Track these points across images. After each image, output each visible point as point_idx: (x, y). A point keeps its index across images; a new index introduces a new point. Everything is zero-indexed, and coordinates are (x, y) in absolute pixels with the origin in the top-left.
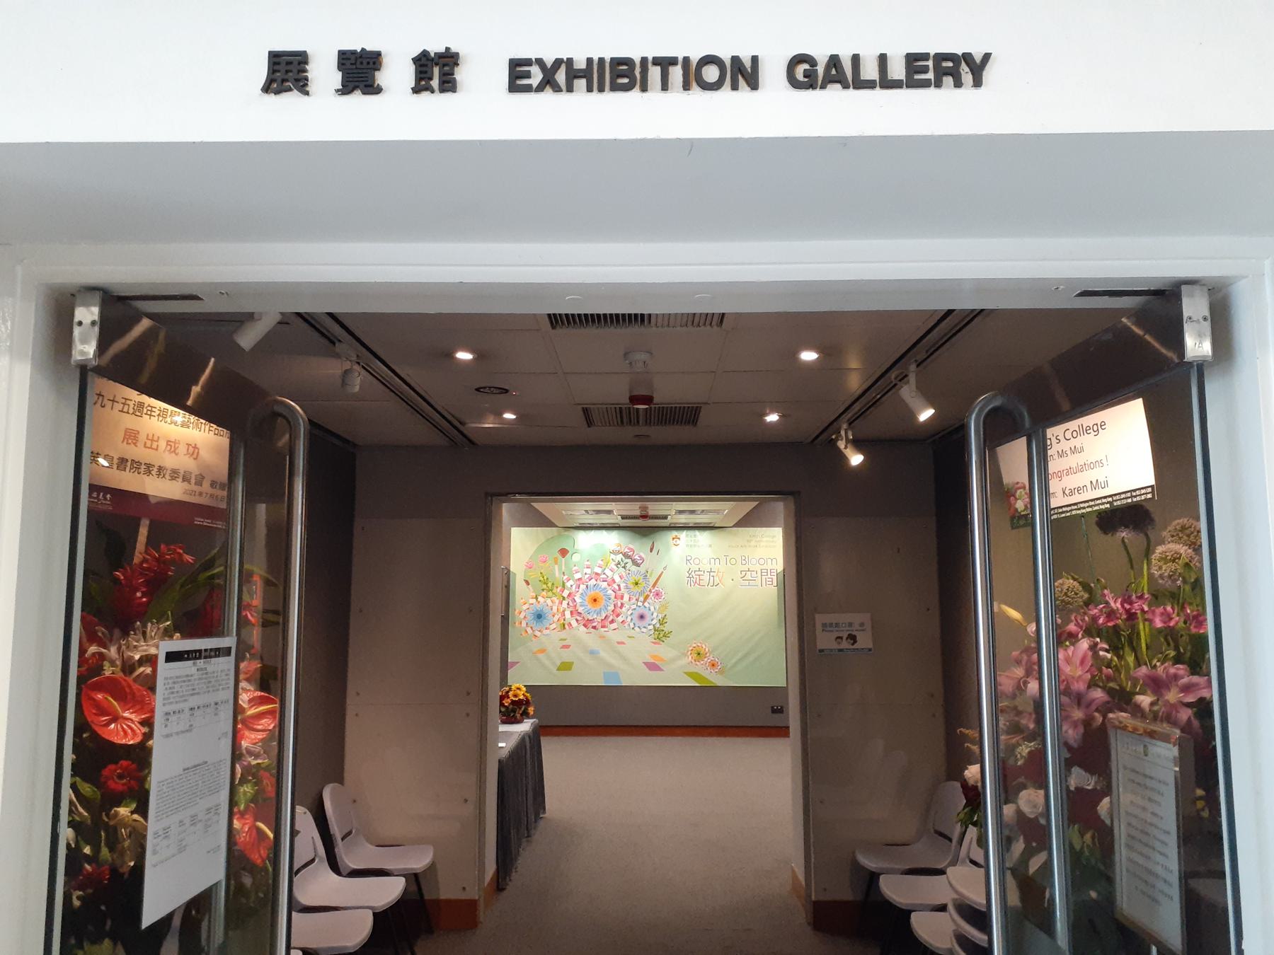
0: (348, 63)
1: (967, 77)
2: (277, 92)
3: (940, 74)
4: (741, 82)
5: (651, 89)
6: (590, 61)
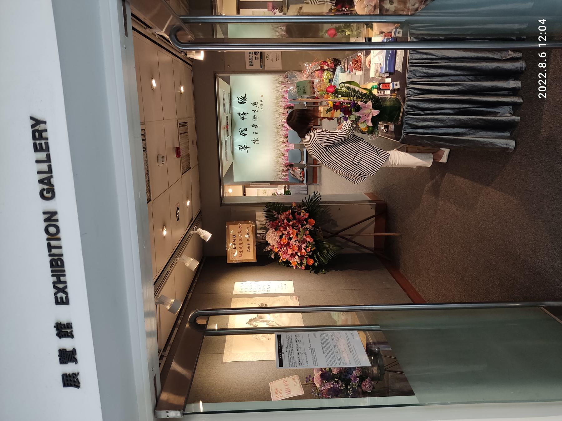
1: (41, 127)
2: (79, 383)
3: (41, 138)
4: (54, 218)
5: (62, 252)
6: (53, 276)
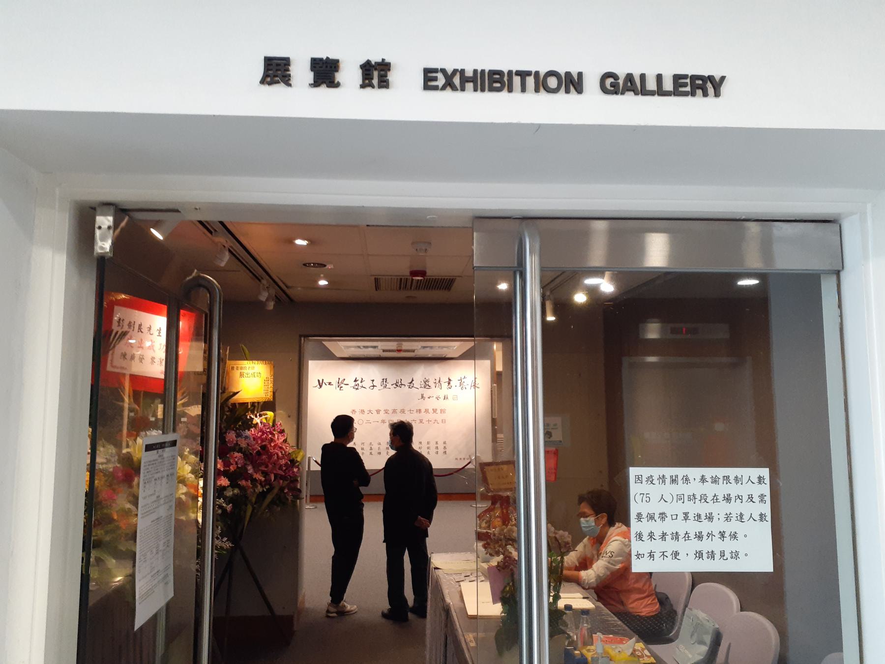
0: (317, 66)
1: (711, 90)
2: (270, 84)
4: (572, 88)
6: (475, 71)
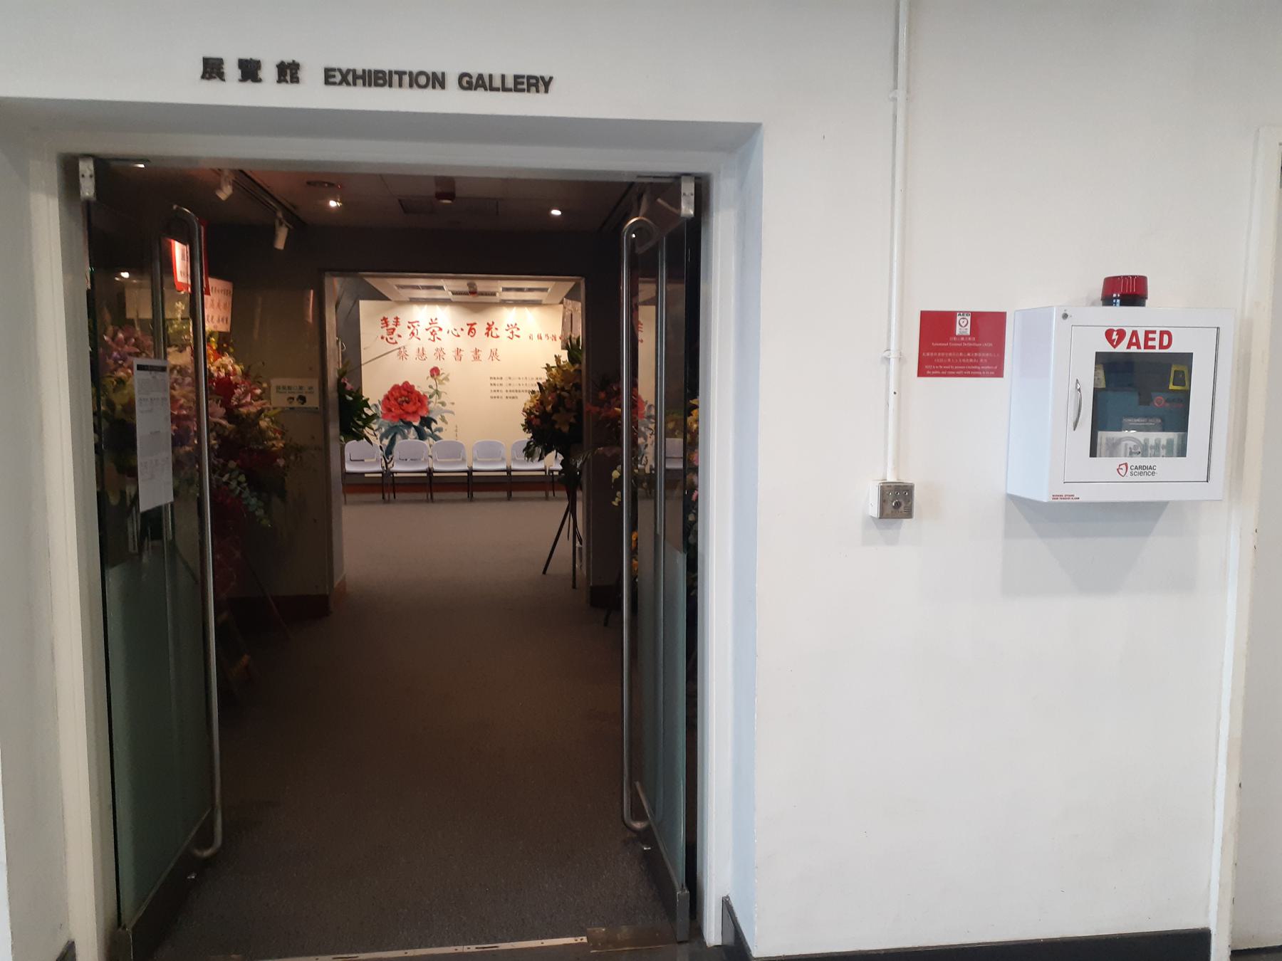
2: (208, 79)
4: (437, 85)
